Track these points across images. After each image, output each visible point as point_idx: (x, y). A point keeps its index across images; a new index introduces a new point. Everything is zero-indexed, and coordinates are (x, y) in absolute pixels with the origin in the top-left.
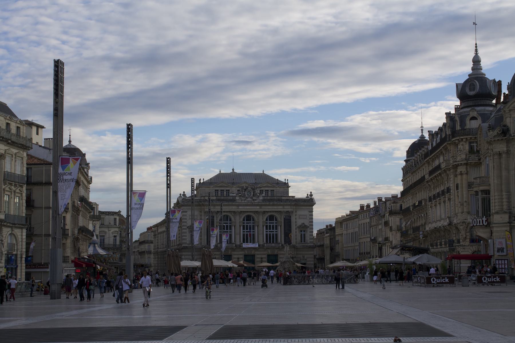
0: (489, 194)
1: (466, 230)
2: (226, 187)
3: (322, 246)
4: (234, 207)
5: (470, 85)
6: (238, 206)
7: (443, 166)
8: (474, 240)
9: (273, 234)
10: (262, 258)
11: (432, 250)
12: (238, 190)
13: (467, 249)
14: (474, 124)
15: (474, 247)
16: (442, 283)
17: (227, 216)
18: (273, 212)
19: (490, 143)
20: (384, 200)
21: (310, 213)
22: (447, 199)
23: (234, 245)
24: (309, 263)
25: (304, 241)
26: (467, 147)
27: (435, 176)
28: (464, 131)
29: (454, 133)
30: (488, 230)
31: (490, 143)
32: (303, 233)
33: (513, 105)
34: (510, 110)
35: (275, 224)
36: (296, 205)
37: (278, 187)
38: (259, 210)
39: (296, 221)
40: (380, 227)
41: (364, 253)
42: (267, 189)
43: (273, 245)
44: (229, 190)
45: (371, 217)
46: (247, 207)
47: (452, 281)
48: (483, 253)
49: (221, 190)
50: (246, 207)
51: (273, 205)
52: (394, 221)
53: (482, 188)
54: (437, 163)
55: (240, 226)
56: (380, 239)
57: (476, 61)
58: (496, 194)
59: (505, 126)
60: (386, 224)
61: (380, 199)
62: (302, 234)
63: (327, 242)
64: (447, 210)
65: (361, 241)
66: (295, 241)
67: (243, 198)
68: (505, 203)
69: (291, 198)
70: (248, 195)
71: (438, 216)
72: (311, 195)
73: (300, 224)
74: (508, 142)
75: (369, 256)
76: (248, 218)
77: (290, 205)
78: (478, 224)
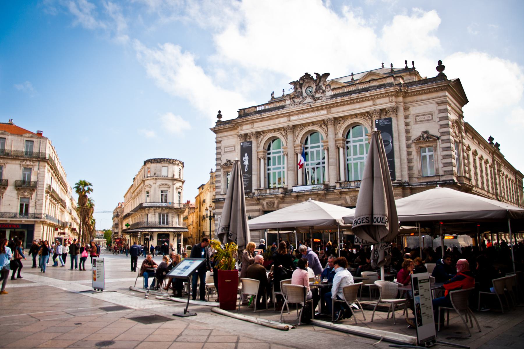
4: (282, 120)
6: (289, 115)
18: (356, 116)
38: (326, 117)
51: (352, 102)
66: (406, 173)
73: (419, 134)
77: (387, 95)
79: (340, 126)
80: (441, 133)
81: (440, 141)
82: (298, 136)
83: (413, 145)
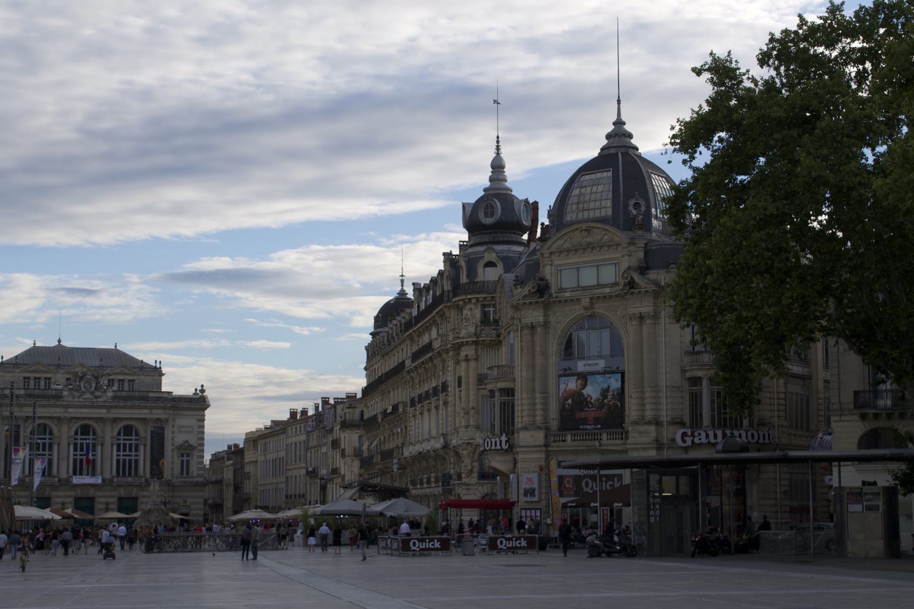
0: (513, 395)
1: (473, 457)
2: (45, 372)
3: (219, 482)
4: (58, 410)
5: (486, 208)
6: (67, 407)
7: (436, 345)
8: (486, 475)
9: (130, 461)
10: (107, 504)
11: (414, 492)
12: (67, 379)
13: (473, 490)
14: (491, 275)
15: (485, 487)
16: (429, 549)
17: (45, 426)
18: (132, 419)
19: (516, 308)
20: (332, 402)
21: (200, 424)
22: (441, 402)
23: (56, 479)
24: (195, 512)
25: (188, 473)
26: (478, 313)
27: (423, 363)
28: (475, 287)
29: (457, 288)
30: (509, 457)
31: (516, 308)
32: (185, 458)
33: (556, 245)
34: (551, 253)
35: (134, 442)
36: (174, 408)
37: (143, 374)
39: (174, 438)
40: (324, 450)
41: (295, 496)
42: (121, 377)
43: (129, 479)
44: (50, 379)
45: (308, 432)
46: (84, 410)
47: (445, 546)
48: (500, 497)
49: (35, 378)
50: (80, 410)
52: (350, 439)
53: (501, 385)
54: (426, 339)
55: (69, 444)
56: (323, 472)
57: (498, 166)
58: (524, 396)
59: (542, 279)
60: (335, 444)
61: (325, 401)
62: (183, 461)
63: (228, 475)
64: (441, 422)
65: (290, 474)
66: (170, 473)
67: (76, 394)
68: (539, 412)
69: (165, 395)
70: (85, 387)
71: (425, 432)
72: (203, 391)
74: (547, 307)
75: (303, 500)
76: (85, 430)
77: (164, 408)
78: (493, 447)
83: (176, 451)
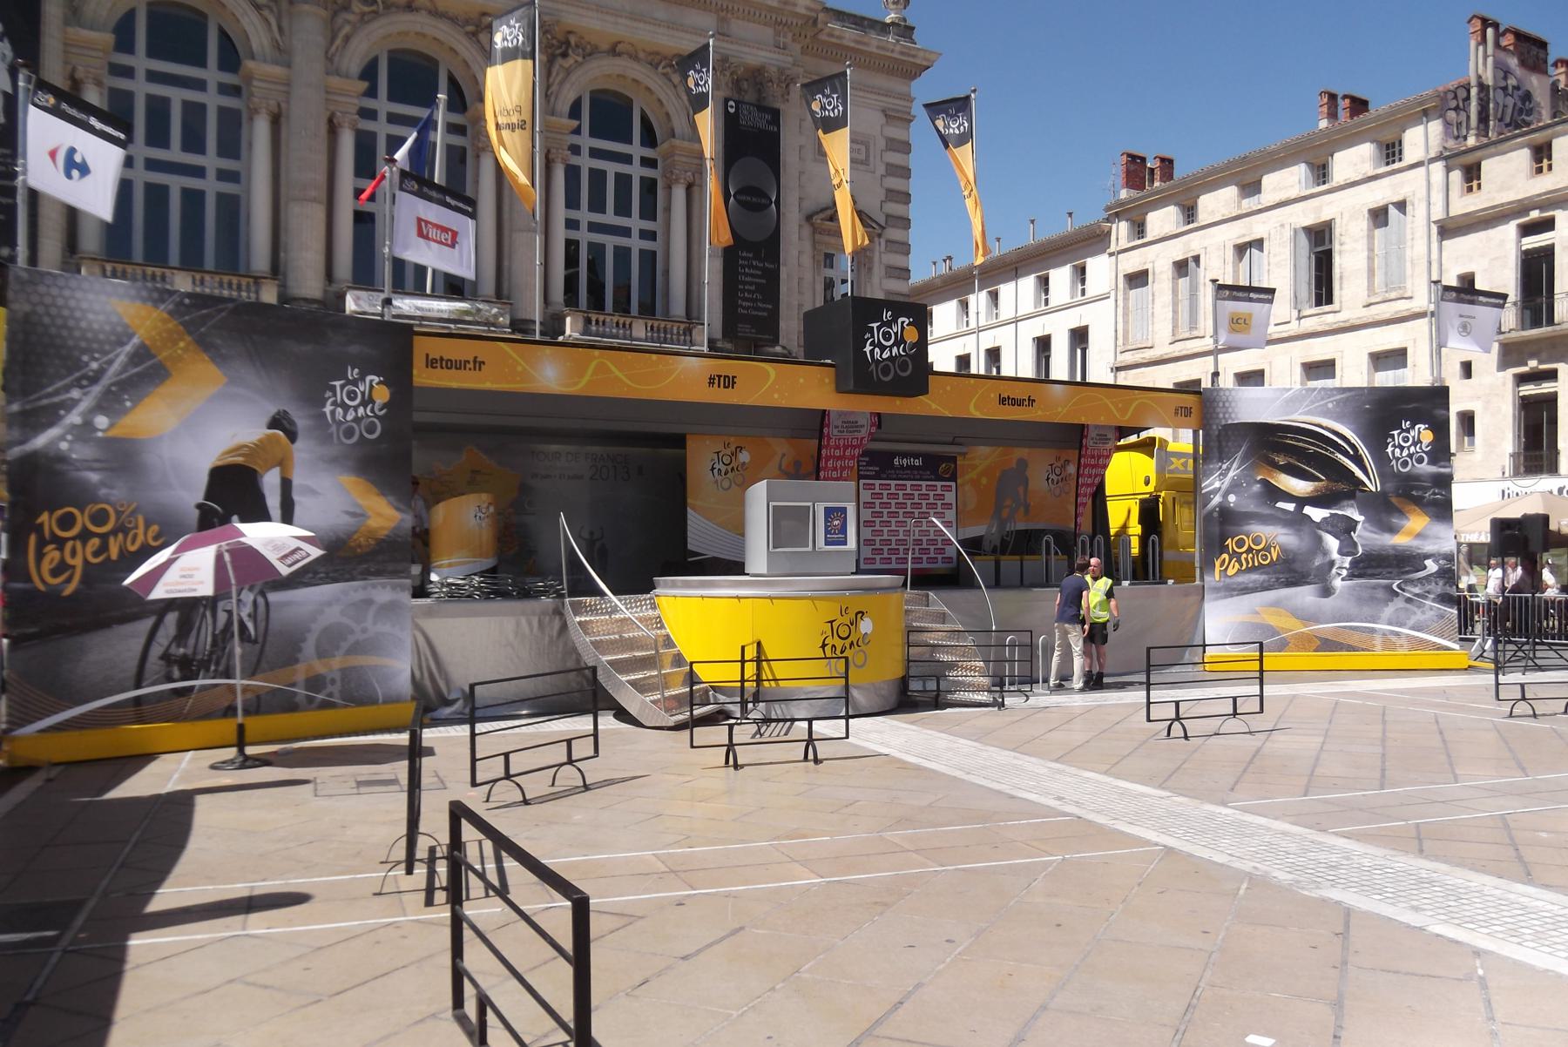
9: (622, 254)
21: (895, 132)
55: (333, 130)
79: (568, 72)
80: (888, 216)
81: (883, 241)
82: (347, 39)
